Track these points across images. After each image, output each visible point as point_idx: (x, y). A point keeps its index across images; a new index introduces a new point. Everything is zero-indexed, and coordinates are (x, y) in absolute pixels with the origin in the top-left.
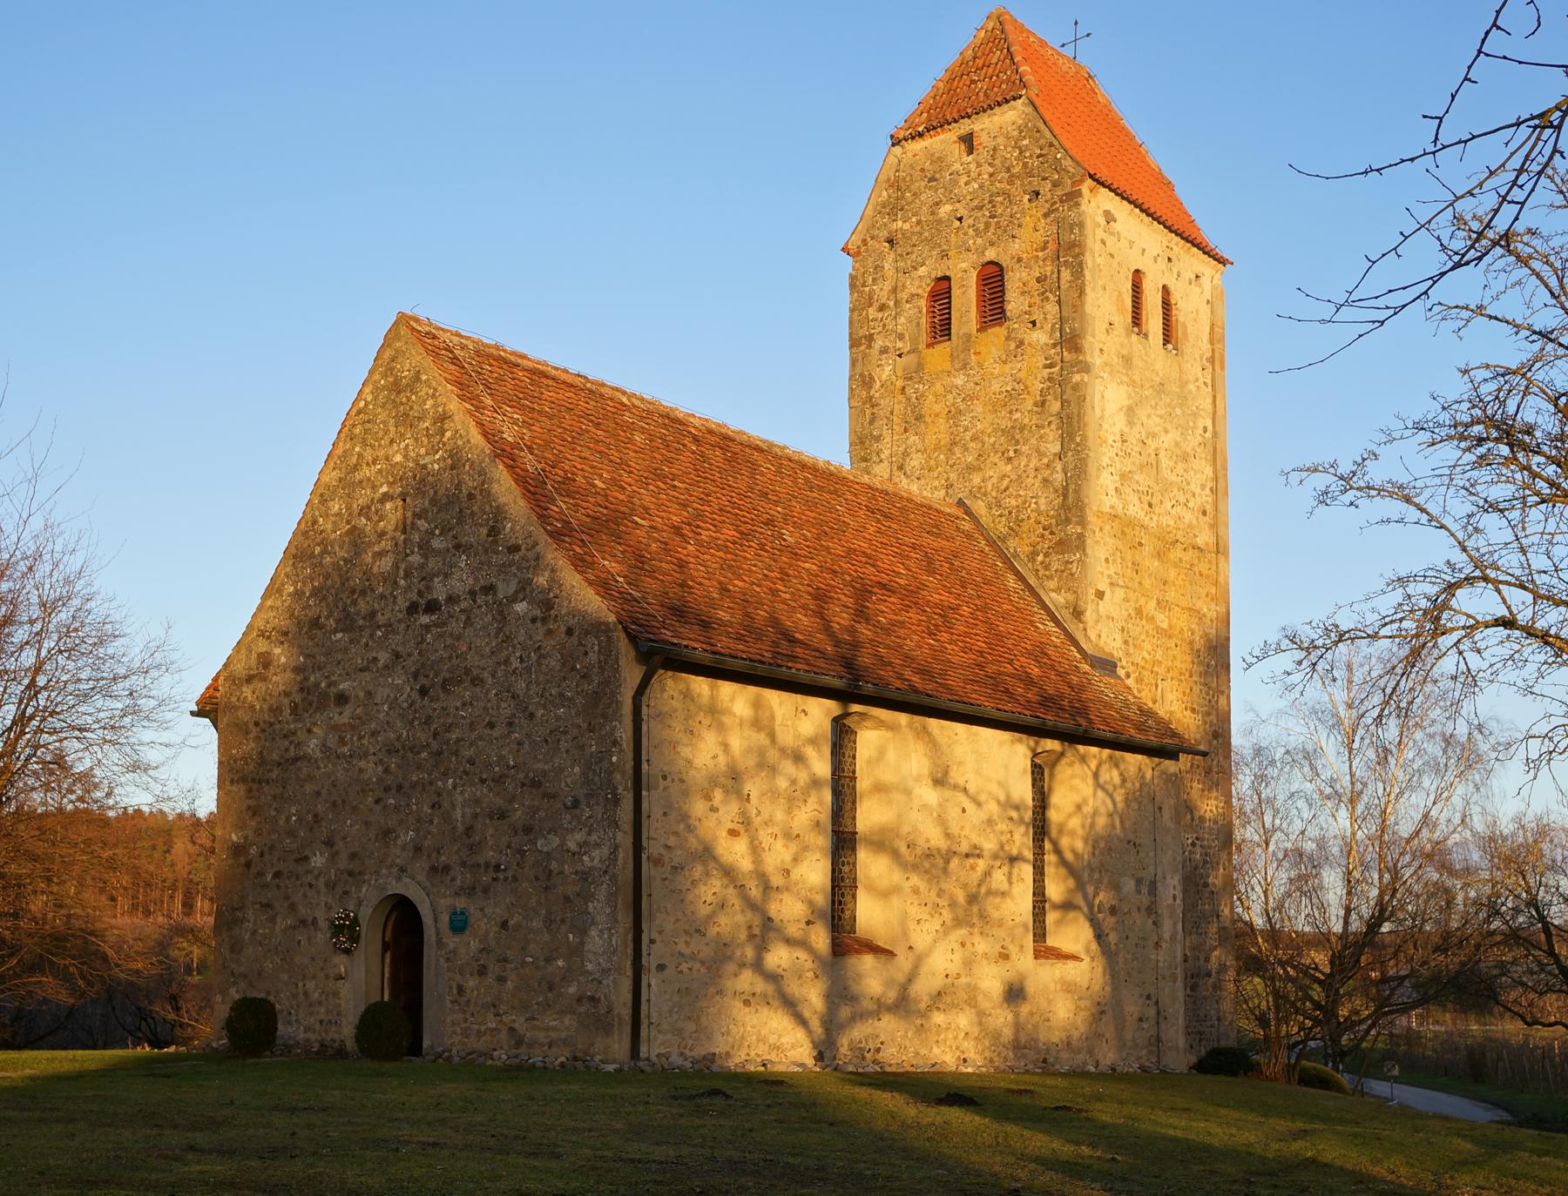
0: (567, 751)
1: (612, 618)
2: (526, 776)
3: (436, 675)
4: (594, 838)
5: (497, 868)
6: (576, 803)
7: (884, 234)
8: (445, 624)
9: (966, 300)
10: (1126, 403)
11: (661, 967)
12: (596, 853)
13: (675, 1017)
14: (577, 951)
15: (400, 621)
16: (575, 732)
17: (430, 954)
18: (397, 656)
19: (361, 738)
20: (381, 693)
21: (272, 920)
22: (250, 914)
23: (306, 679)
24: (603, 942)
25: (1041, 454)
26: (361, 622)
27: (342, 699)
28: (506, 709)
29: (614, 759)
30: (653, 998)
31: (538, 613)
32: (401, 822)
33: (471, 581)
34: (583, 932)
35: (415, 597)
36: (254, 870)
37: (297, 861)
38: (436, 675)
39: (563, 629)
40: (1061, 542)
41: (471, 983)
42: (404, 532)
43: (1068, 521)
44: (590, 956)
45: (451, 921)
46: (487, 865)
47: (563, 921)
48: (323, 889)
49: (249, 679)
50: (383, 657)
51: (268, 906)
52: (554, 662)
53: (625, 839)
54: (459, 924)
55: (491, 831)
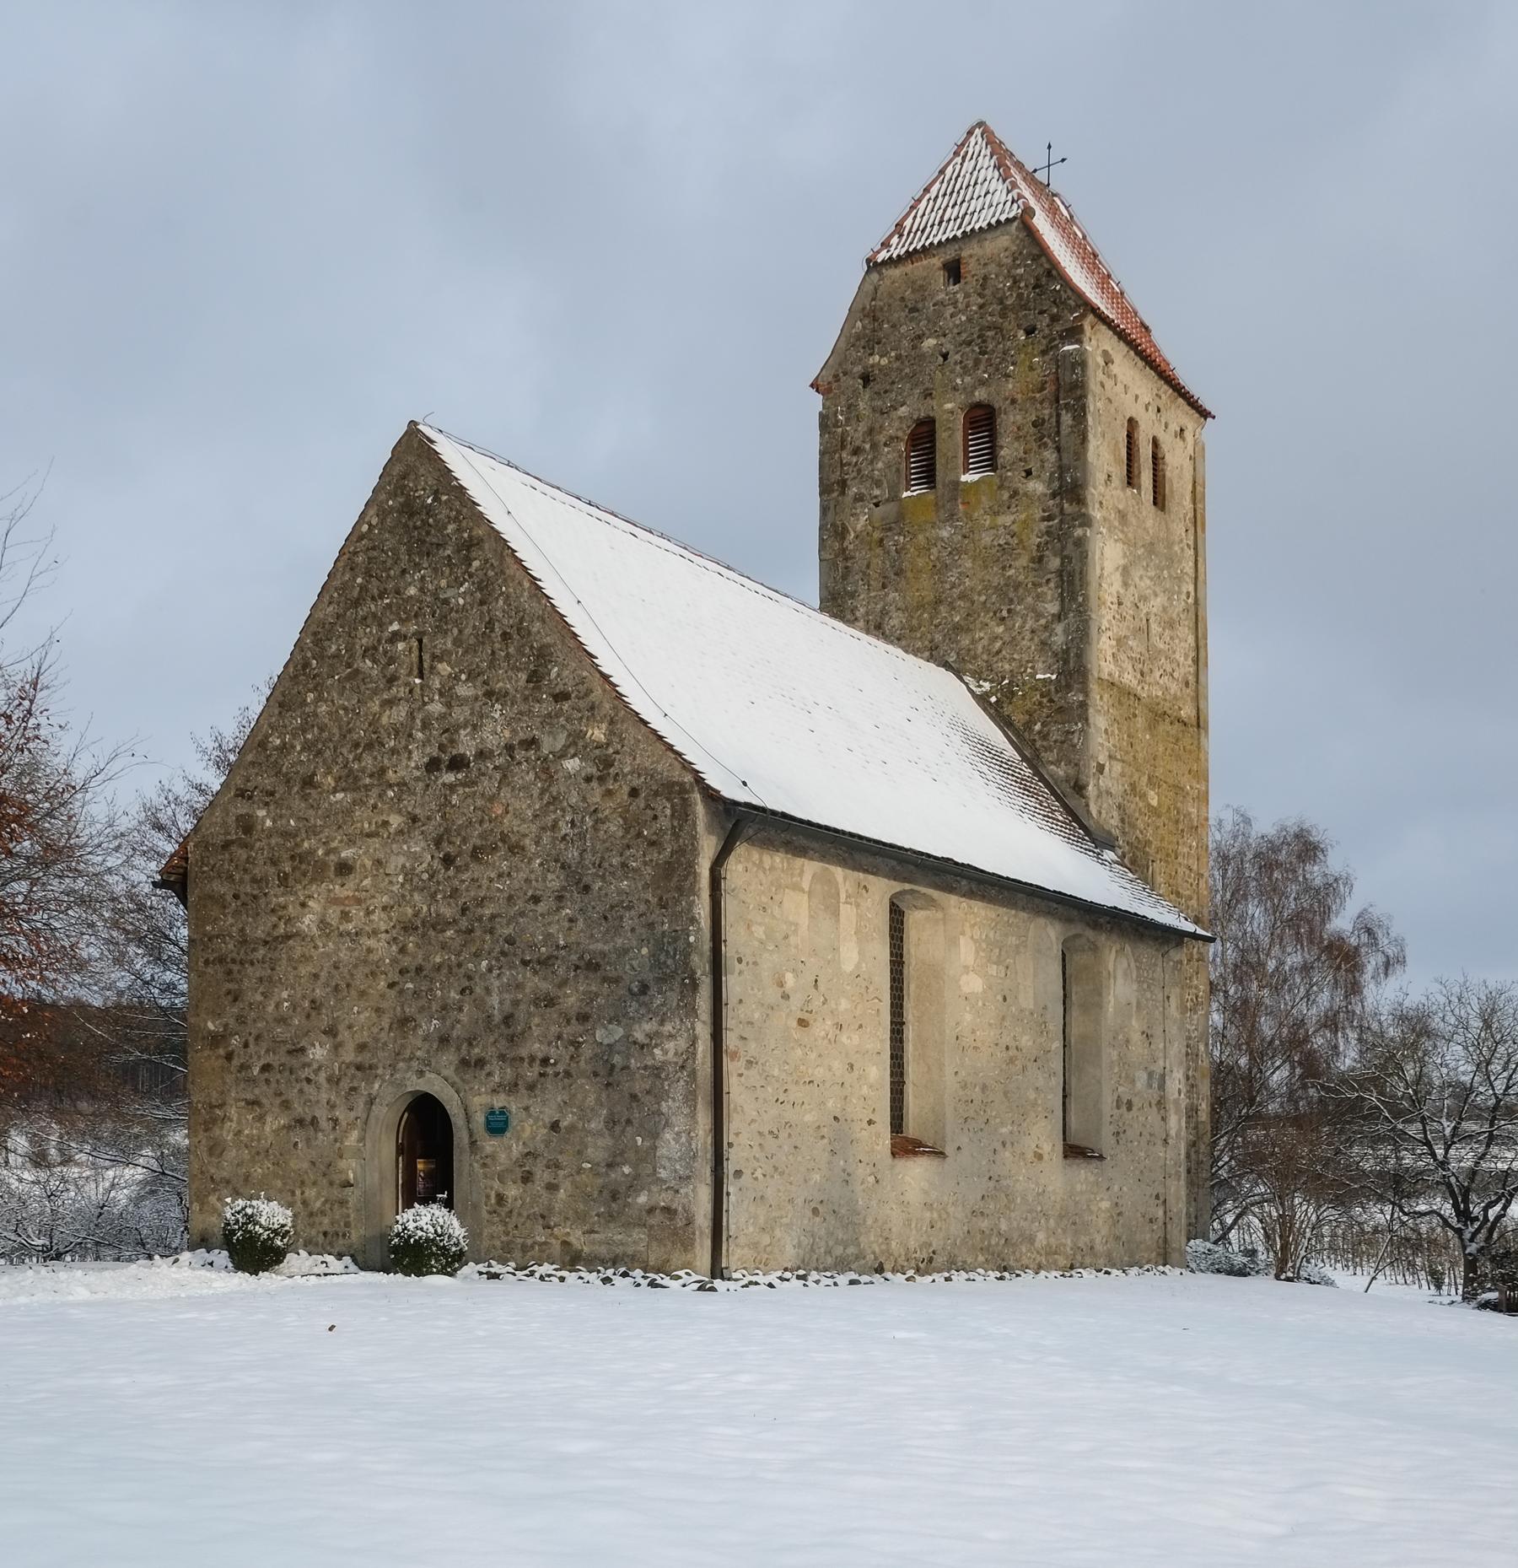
0: (633, 930)
2: (581, 958)
3: (464, 841)
4: (668, 1028)
5: (545, 1061)
6: (644, 989)
8: (474, 783)
10: (1122, 562)
12: (670, 1046)
14: (648, 1156)
15: (417, 779)
16: (643, 908)
19: (368, 913)
20: (396, 863)
21: (261, 1119)
22: (233, 1112)
26: (367, 781)
27: (344, 869)
28: (554, 881)
29: (692, 939)
32: (421, 1010)
33: (507, 734)
34: (655, 1135)
36: (236, 1062)
37: (289, 1052)
38: (464, 841)
39: (626, 789)
41: (512, 1191)
42: (421, 676)
43: (1069, 687)
44: (664, 1162)
45: (488, 1122)
46: (532, 1059)
49: (226, 846)
51: (254, 1103)
52: (614, 827)
53: (703, 1031)
54: (498, 1124)
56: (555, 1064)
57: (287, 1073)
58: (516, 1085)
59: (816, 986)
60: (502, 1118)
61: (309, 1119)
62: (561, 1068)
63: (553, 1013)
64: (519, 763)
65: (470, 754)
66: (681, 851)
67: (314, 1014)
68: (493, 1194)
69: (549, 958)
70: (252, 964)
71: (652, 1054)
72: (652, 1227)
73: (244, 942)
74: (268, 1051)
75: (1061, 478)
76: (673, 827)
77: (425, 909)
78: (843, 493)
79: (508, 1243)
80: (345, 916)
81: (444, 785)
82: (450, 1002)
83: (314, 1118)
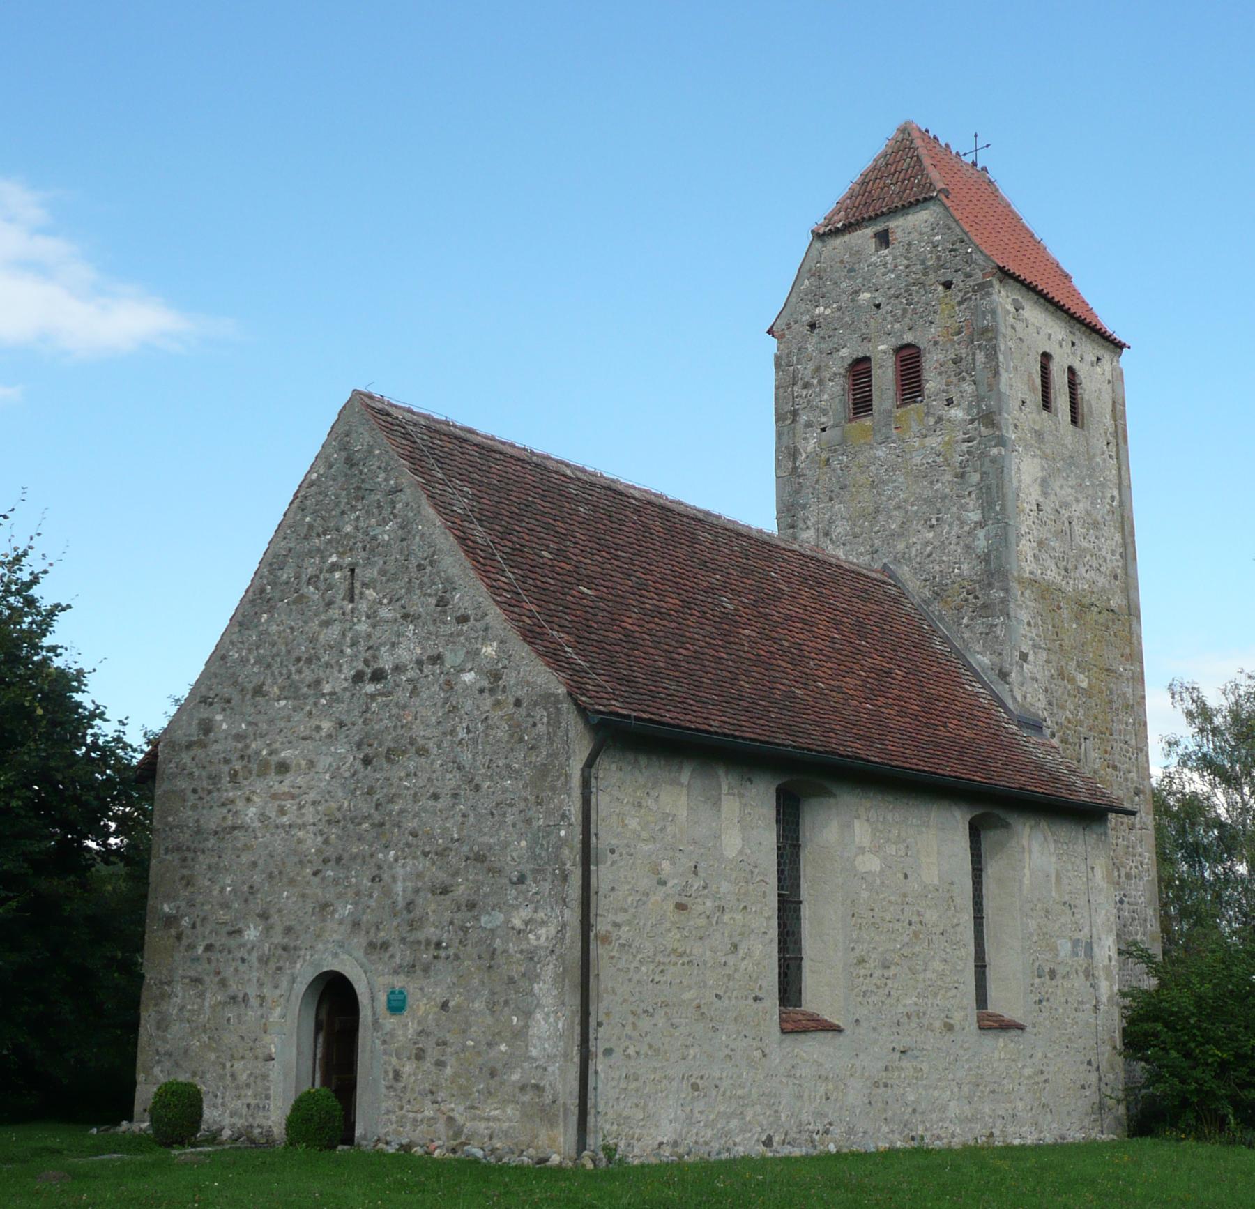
0: (514, 825)
1: (562, 690)
2: (471, 850)
3: (380, 745)
4: (541, 915)
5: (438, 945)
6: (522, 879)
7: (806, 318)
8: (390, 694)
9: (884, 378)
11: (608, 1052)
12: (542, 931)
13: (622, 1104)
14: (520, 1035)
15: (345, 689)
16: (522, 805)
17: (366, 1039)
18: (341, 725)
19: (300, 807)
20: (324, 762)
21: (202, 995)
22: (178, 989)
23: (247, 747)
24: (549, 1025)
25: (963, 523)
27: (283, 768)
28: (452, 780)
29: (562, 833)
30: (600, 1086)
31: (485, 684)
32: (340, 896)
33: (418, 651)
34: (527, 1014)
35: (361, 666)
36: (185, 942)
37: (230, 933)
38: (380, 745)
39: (512, 700)
45: (389, 1001)
46: (428, 943)
47: (506, 1003)
48: (256, 964)
49: (189, 746)
50: (326, 725)
51: (197, 981)
52: (501, 733)
53: (572, 916)
54: (397, 1005)
55: (433, 906)
56: (446, 948)
57: (225, 953)
58: (414, 966)
59: (696, 873)
60: (400, 997)
61: (241, 995)
62: (451, 951)
63: (447, 900)
64: (427, 676)
65: (388, 667)
66: (554, 755)
67: (251, 897)
68: (390, 1069)
69: (445, 850)
70: (203, 852)
71: (527, 939)
72: (523, 1103)
73: (198, 832)
74: (211, 932)
75: (978, 406)
76: (549, 733)
77: (346, 804)
79: (403, 1117)
80: (282, 811)
81: (367, 694)
82: (362, 888)
83: (246, 995)
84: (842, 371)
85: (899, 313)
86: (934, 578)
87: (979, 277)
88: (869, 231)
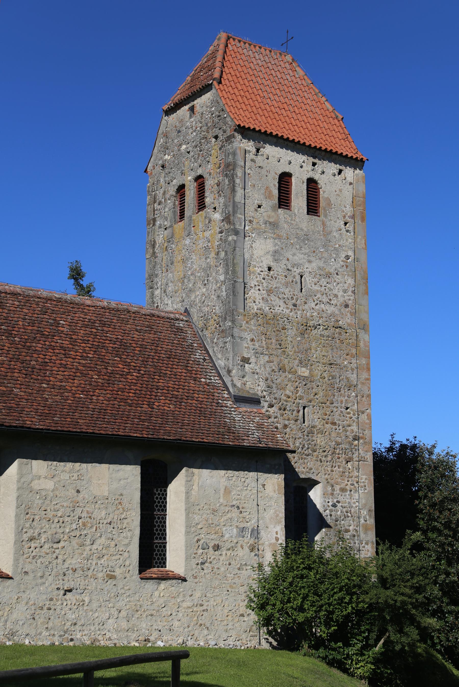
7: (160, 162)
40: (223, 331)
78: (154, 225)
84: (174, 194)
85: (197, 156)
86: (205, 315)
87: (229, 133)
88: (187, 107)
